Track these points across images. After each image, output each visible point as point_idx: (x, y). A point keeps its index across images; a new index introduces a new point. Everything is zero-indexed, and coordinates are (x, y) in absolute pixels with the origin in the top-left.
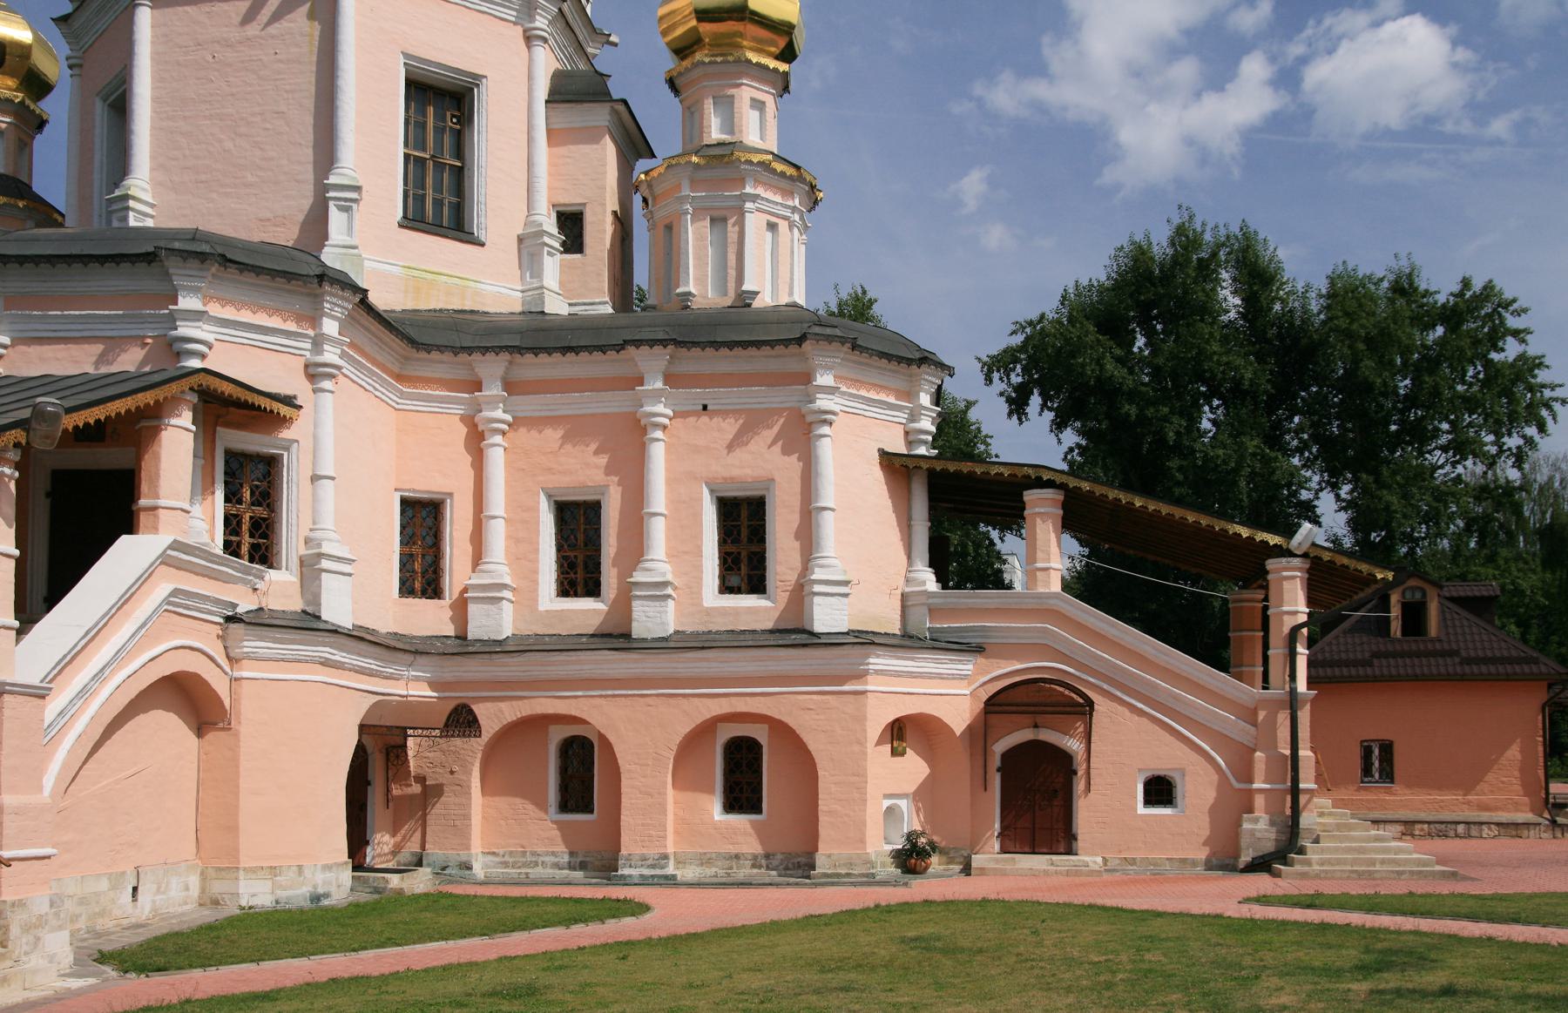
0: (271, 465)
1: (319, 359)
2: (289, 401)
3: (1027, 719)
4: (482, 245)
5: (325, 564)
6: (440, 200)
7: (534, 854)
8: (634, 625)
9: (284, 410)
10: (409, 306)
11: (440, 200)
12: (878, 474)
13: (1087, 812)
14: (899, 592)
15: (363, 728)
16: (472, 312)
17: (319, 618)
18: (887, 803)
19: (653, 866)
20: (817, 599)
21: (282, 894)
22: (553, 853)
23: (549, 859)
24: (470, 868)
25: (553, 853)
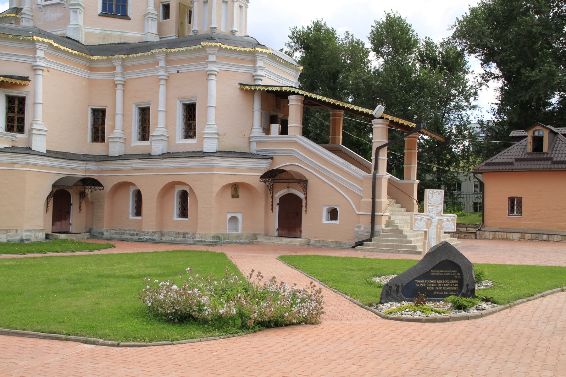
0: (22, 101)
1: (36, 64)
2: (26, 79)
3: (286, 185)
4: (130, 19)
5: (34, 132)
7: (124, 230)
8: (152, 150)
9: (23, 82)
10: (101, 43)
12: (238, 92)
13: (306, 220)
14: (248, 136)
15: (54, 186)
16: (124, 43)
17: (31, 149)
18: (229, 216)
19: (150, 236)
20: (205, 140)
21: (10, 239)
22: (129, 230)
23: (128, 232)
24: (103, 234)
25: (129, 230)
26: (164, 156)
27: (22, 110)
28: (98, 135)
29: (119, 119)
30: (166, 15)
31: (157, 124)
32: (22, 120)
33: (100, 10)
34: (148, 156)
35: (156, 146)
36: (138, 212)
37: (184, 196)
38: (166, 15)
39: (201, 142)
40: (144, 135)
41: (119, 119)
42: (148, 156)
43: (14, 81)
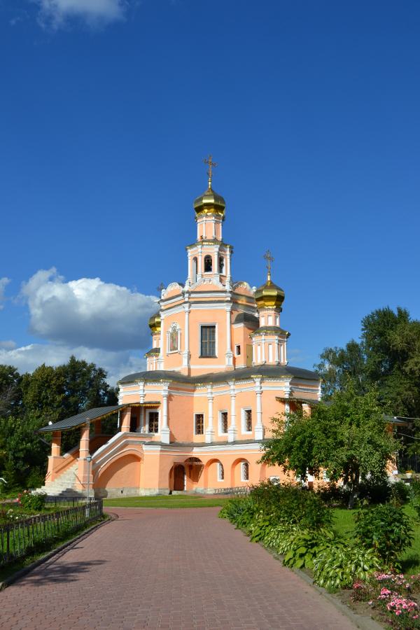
6: (207, 351)
11: (207, 351)
26: (235, 443)
27: (157, 420)
28: (200, 430)
29: (210, 420)
30: (239, 353)
31: (230, 423)
32: (157, 426)
33: (199, 355)
34: (226, 443)
35: (230, 437)
36: (223, 478)
37: (247, 465)
38: (239, 353)
39: (254, 434)
40: (225, 431)
41: (210, 420)
42: (226, 443)
43: (153, 405)
